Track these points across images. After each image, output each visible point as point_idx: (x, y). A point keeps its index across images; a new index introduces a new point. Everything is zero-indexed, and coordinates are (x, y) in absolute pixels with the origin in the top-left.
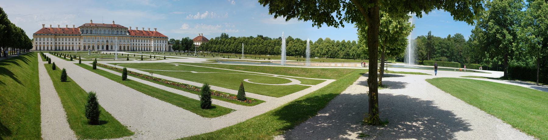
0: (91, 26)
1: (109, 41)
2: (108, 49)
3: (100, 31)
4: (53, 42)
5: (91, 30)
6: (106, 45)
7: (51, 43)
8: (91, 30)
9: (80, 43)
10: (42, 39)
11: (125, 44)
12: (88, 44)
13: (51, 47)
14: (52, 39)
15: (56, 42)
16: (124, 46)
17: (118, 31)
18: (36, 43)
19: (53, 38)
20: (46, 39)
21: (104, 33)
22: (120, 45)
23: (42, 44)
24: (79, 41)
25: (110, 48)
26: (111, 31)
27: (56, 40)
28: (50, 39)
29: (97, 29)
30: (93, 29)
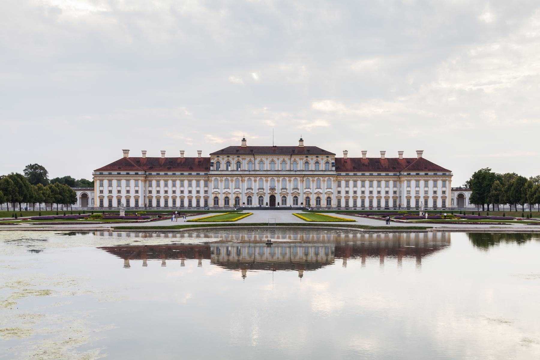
0: (239, 153)
1: (279, 186)
2: (275, 205)
3: (261, 162)
4: (141, 188)
5: (239, 163)
6: (269, 195)
7: (137, 192)
8: (239, 163)
10: (114, 182)
11: (321, 193)
12: (224, 193)
13: (137, 202)
14: (138, 183)
15: (150, 189)
16: (318, 198)
17: (307, 163)
18: (101, 192)
19: (140, 182)
20: (123, 182)
21: (271, 167)
22: (305, 196)
23: (115, 194)
24: (206, 185)
26: (288, 162)
27: (151, 186)
28: (132, 182)
29: (253, 159)
30: (243, 159)
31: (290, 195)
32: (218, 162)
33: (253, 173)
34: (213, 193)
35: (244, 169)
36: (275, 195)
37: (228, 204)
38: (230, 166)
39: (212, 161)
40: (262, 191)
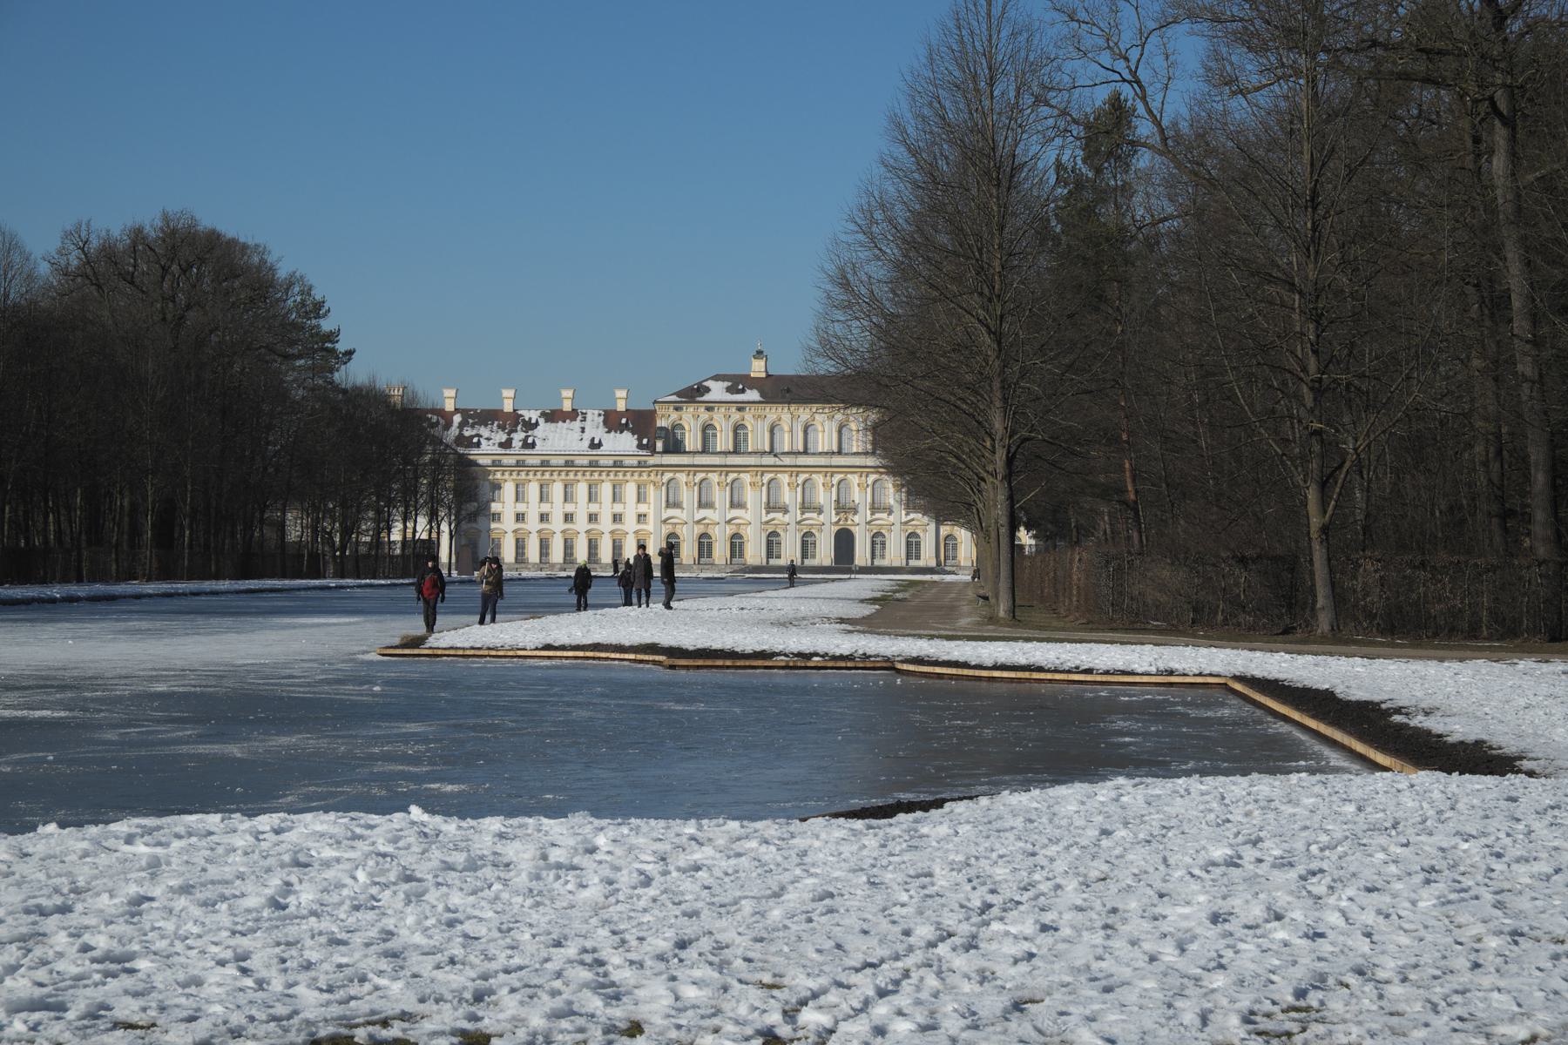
5: (738, 429)
8: (738, 429)
9: (641, 517)
12: (698, 522)
15: (472, 506)
24: (640, 498)
25: (862, 556)
29: (786, 417)
31: (896, 528)
32: (678, 426)
33: (787, 460)
34: (665, 521)
35: (760, 448)
36: (852, 528)
37: (710, 555)
38: (715, 436)
39: (661, 423)
40: (814, 515)
